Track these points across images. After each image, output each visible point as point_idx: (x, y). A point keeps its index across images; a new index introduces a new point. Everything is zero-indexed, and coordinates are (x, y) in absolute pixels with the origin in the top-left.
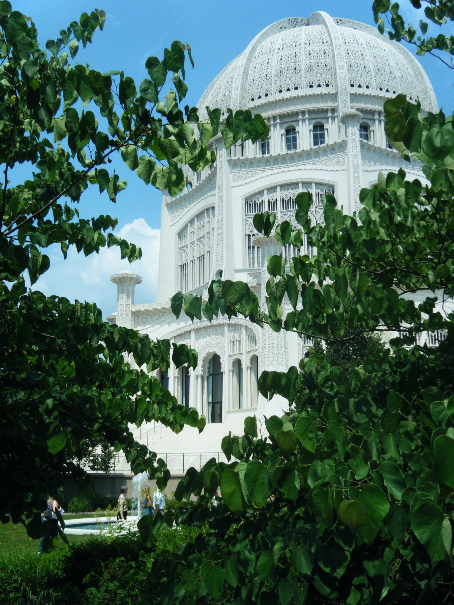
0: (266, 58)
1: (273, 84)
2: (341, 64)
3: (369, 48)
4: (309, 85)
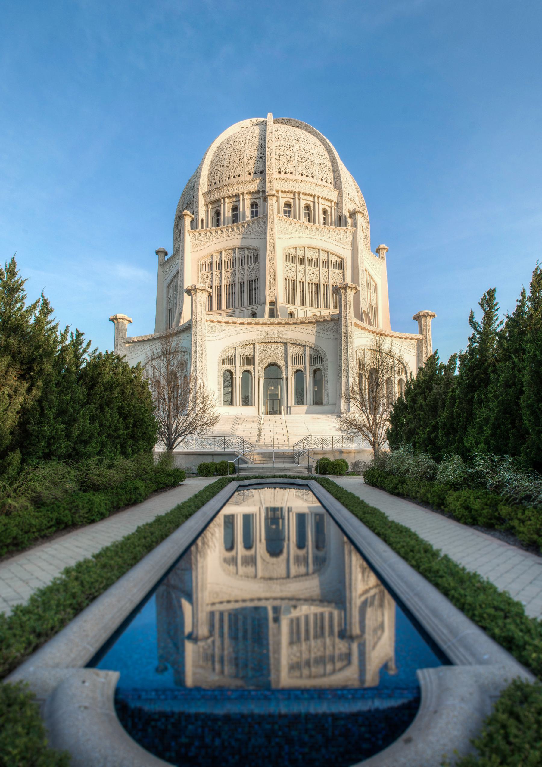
4: (248, 173)
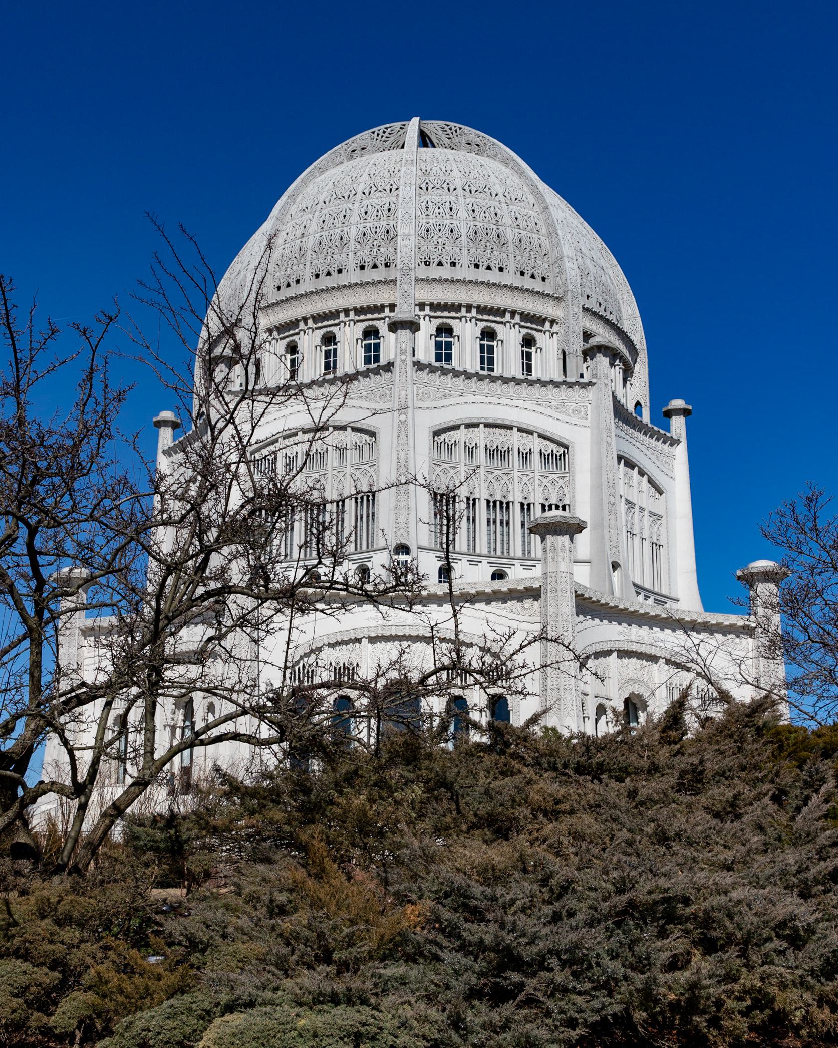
1: (308, 264)
2: (407, 232)
3: (467, 194)
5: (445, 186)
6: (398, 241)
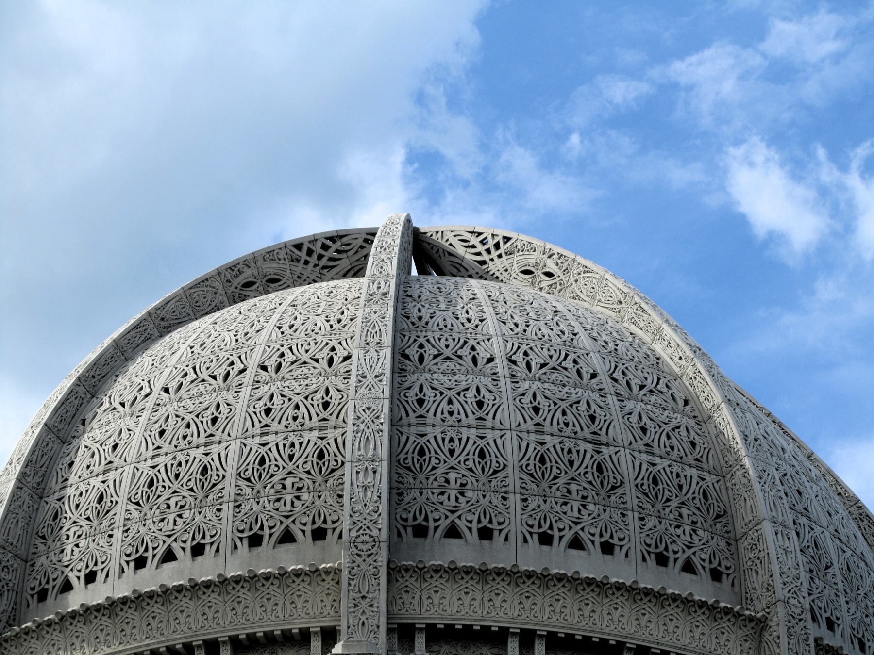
0: (114, 427)
1: (118, 533)
5: (465, 352)
6: (347, 479)
